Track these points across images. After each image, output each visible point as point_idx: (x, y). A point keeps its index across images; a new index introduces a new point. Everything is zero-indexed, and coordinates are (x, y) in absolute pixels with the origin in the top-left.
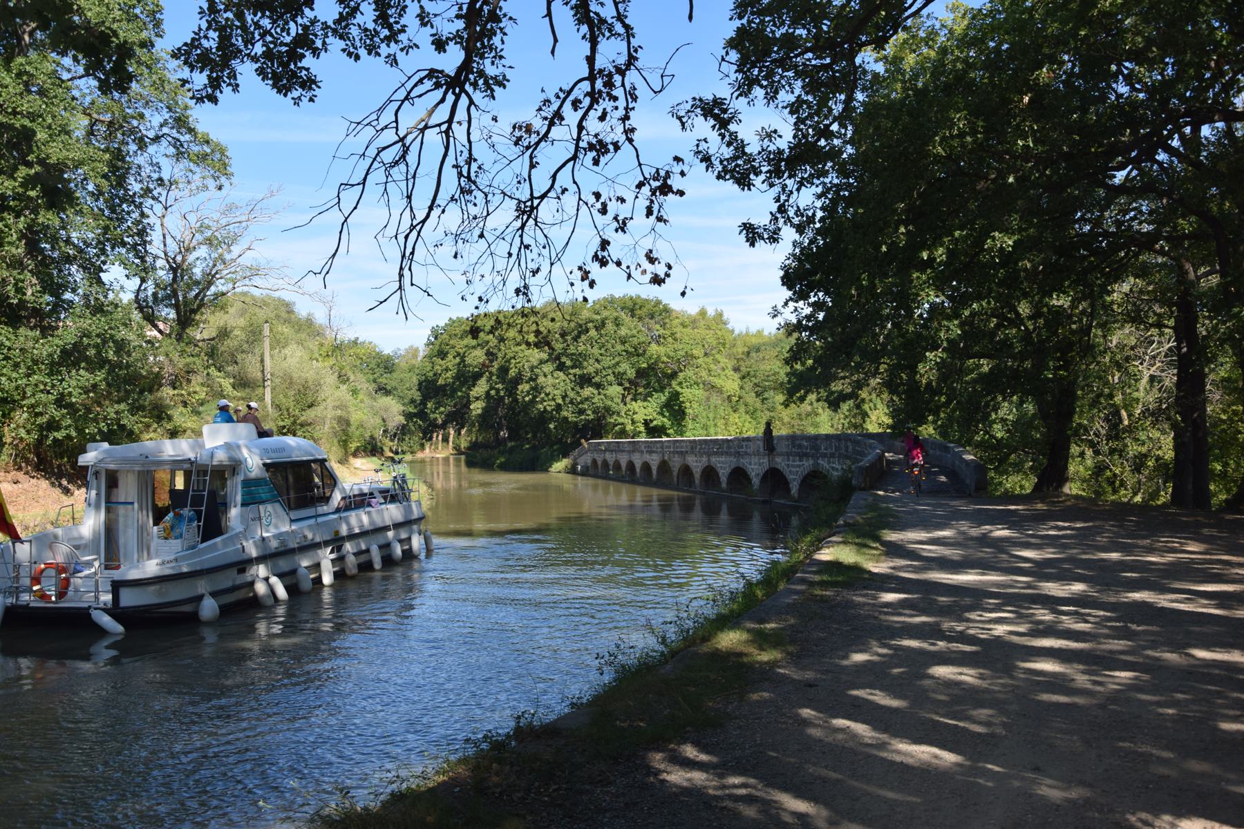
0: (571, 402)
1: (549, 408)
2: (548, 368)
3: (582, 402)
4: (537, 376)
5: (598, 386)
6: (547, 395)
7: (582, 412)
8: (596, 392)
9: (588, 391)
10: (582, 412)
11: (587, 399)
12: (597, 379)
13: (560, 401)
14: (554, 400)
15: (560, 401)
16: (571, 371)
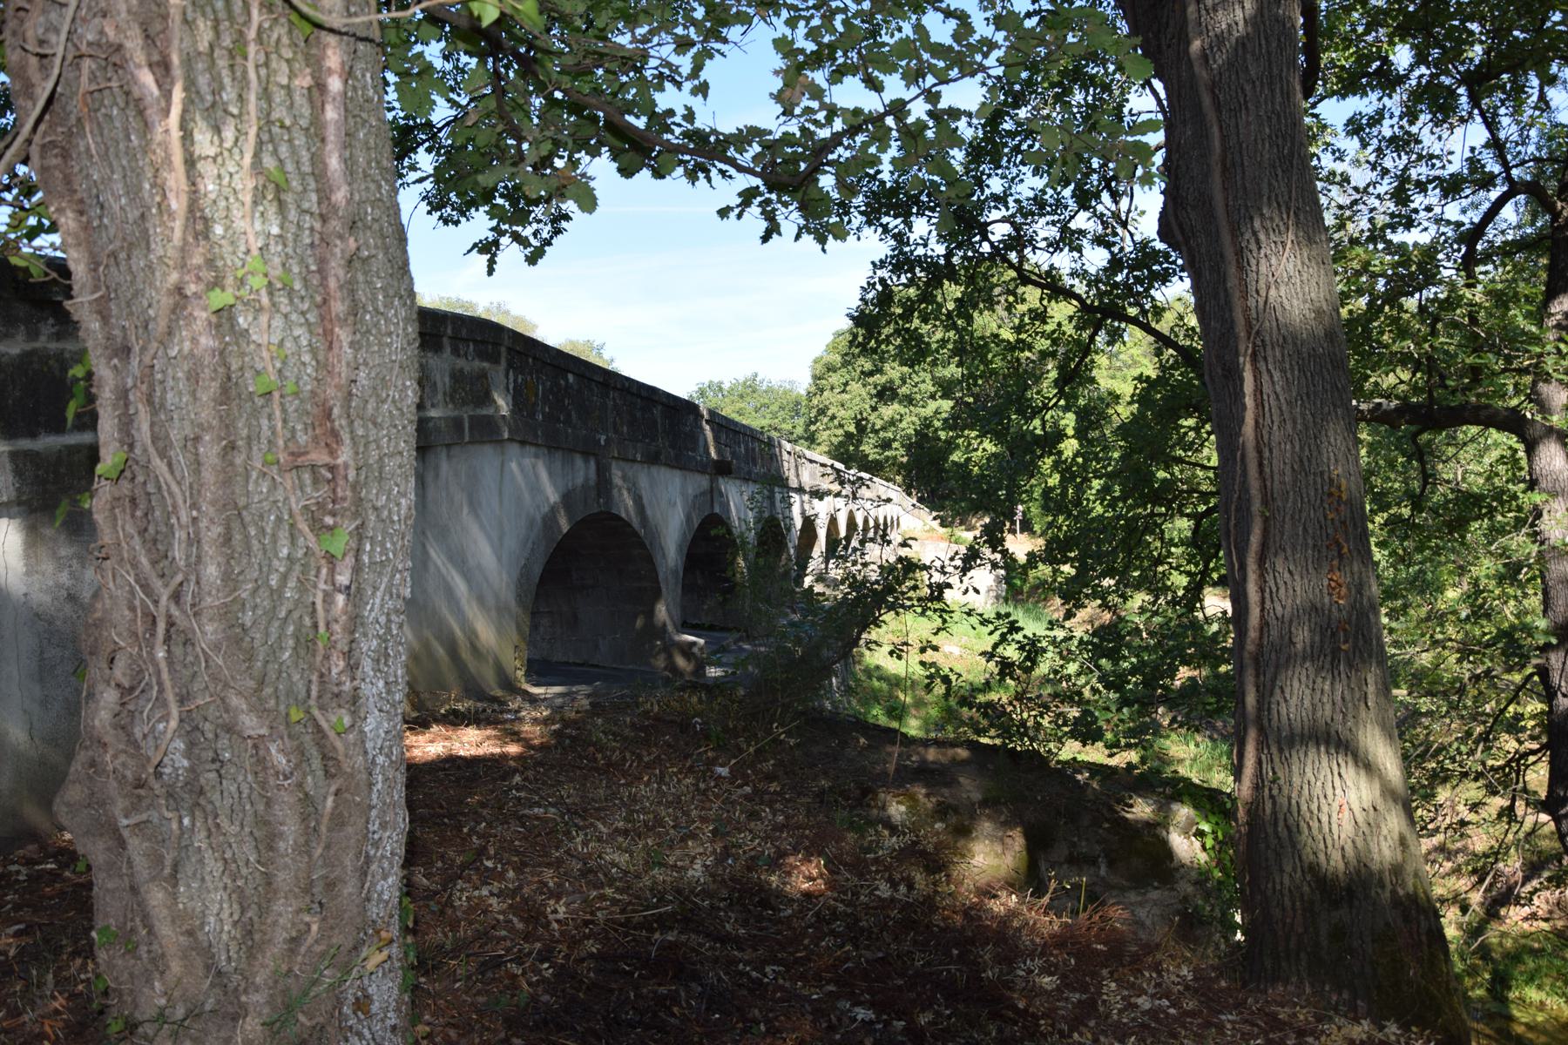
0: (877, 432)
1: (834, 439)
2: (835, 379)
3: (883, 428)
4: (822, 391)
5: (909, 400)
6: (833, 417)
7: (886, 445)
8: (903, 410)
9: (888, 411)
10: (886, 445)
11: (892, 423)
12: (904, 390)
13: (852, 429)
14: (841, 426)
15: (852, 429)
16: (871, 380)
